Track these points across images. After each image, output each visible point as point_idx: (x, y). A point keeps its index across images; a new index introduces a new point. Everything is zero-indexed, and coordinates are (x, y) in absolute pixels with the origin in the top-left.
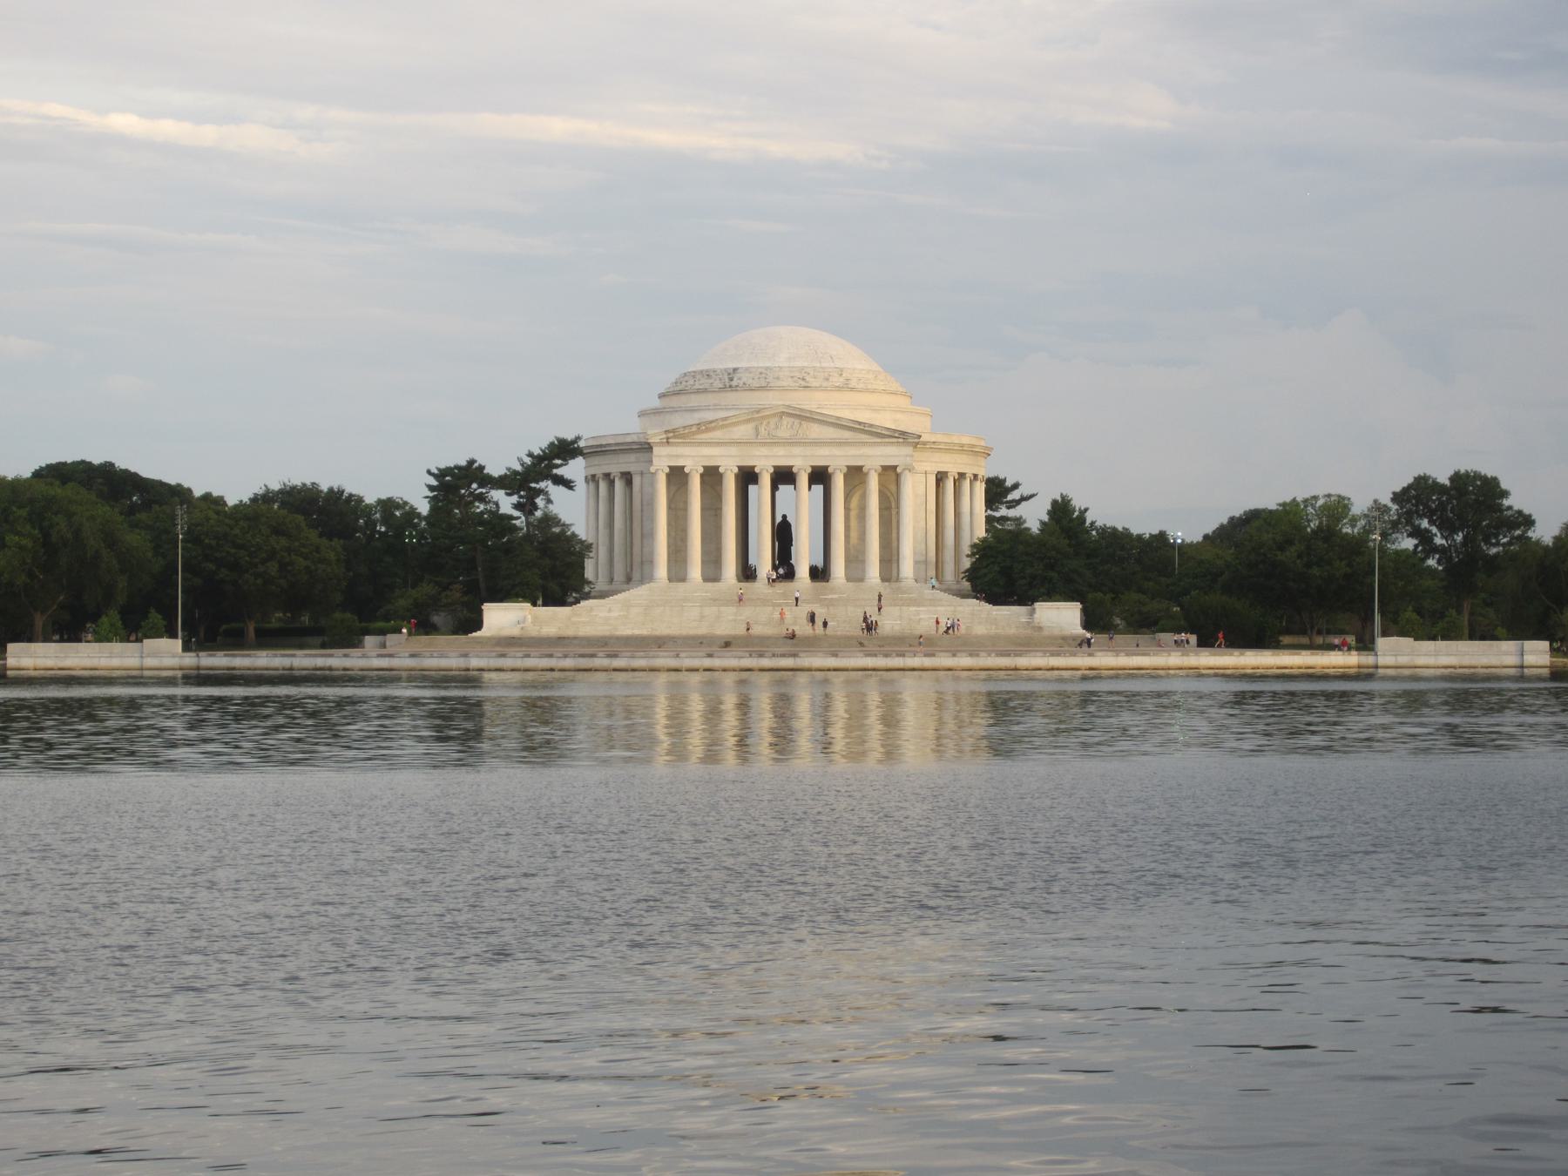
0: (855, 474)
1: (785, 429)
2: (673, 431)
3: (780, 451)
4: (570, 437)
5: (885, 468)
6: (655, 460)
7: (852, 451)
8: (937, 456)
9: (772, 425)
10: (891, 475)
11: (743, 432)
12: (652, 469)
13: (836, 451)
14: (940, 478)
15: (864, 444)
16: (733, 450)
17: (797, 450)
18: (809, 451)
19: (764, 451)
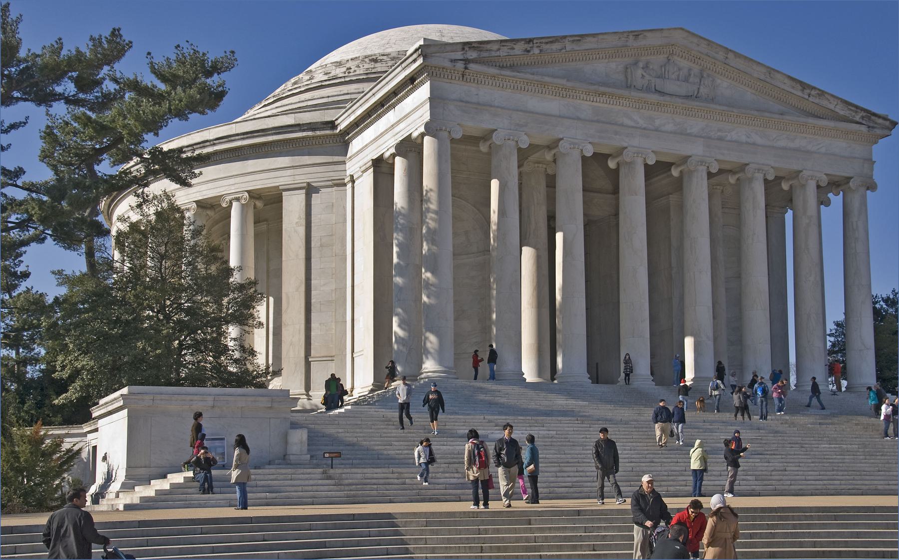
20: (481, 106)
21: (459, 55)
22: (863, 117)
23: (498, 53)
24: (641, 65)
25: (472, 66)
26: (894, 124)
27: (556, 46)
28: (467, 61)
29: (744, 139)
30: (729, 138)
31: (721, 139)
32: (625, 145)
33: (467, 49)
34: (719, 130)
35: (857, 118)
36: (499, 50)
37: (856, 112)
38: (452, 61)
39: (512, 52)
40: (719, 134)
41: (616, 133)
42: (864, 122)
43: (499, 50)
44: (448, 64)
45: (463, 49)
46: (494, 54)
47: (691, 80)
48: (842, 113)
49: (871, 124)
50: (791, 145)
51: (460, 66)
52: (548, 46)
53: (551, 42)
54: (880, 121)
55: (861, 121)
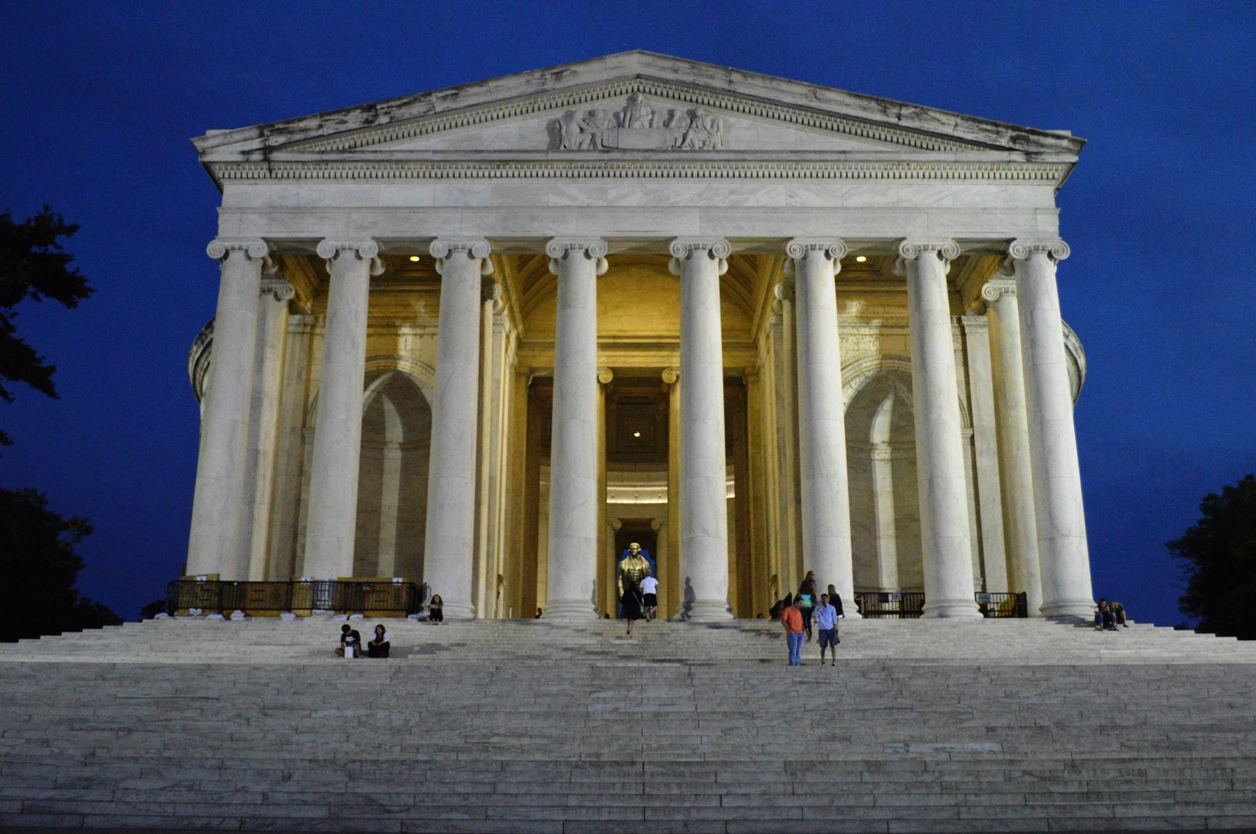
6: (227, 224)
7: (863, 194)
9: (605, 123)
12: (214, 249)
13: (808, 194)
16: (481, 190)
17: (683, 191)
19: (578, 192)
20: (299, 211)
22: (1014, 139)
23: (320, 132)
24: (579, 116)
25: (275, 156)
29: (782, 201)
30: (751, 203)
31: (733, 208)
32: (549, 233)
33: (266, 132)
34: (732, 193)
35: (1003, 142)
36: (320, 126)
37: (998, 133)
38: (243, 153)
39: (343, 128)
40: (732, 198)
41: (533, 218)
42: (1018, 147)
43: (320, 126)
44: (239, 158)
45: (261, 135)
46: (314, 134)
47: (673, 124)
48: (970, 137)
49: (1033, 149)
50: (880, 200)
51: (257, 157)
52: (404, 110)
53: (406, 104)
55: (1011, 145)
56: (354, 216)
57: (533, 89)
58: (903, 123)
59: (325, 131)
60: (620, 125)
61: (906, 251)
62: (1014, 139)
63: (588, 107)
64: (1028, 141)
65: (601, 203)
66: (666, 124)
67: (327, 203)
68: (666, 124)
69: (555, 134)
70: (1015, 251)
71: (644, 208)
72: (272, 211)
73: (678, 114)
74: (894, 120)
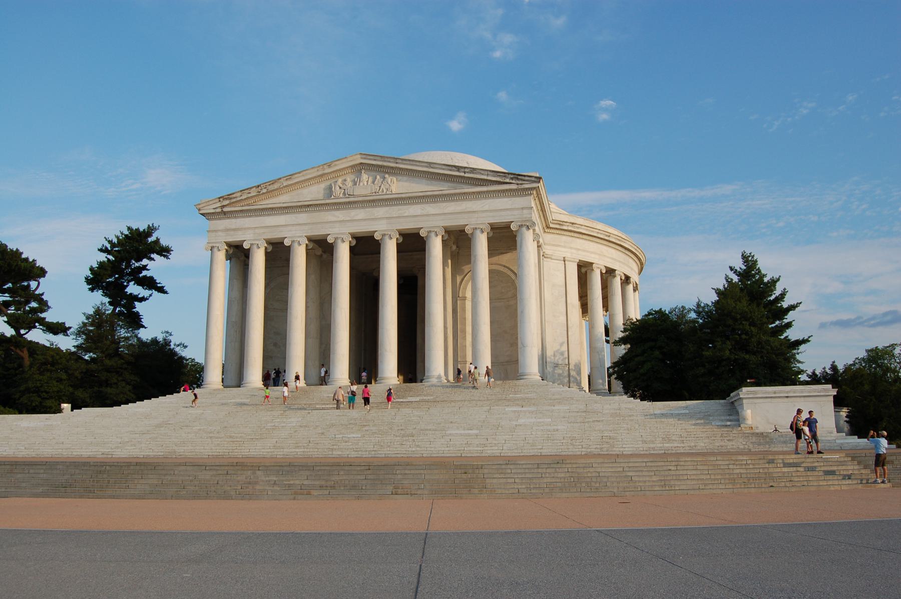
0: (458, 242)
1: (367, 185)
2: (228, 197)
3: (359, 214)
4: (143, 227)
5: (494, 228)
8: (580, 243)
9: (349, 184)
10: (504, 239)
11: (314, 192)
14: (584, 270)
15: (464, 196)
16: (303, 217)
17: (380, 212)
18: (395, 211)
19: (340, 215)
21: (219, 205)
26: (540, 178)
27: (276, 186)
28: (224, 206)
35: (508, 180)
39: (249, 195)
54: (527, 178)
56: (256, 230)
57: (320, 173)
58: (466, 175)
59: (243, 197)
60: (355, 184)
61: (468, 230)
62: (512, 179)
63: (344, 178)
64: (518, 179)
65: (348, 219)
66: (373, 182)
67: (247, 226)
68: (373, 182)
69: (329, 191)
70: (513, 227)
71: (365, 220)
72: (227, 230)
73: (378, 177)
74: (462, 174)
